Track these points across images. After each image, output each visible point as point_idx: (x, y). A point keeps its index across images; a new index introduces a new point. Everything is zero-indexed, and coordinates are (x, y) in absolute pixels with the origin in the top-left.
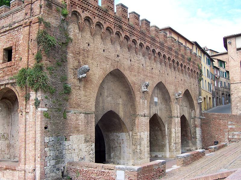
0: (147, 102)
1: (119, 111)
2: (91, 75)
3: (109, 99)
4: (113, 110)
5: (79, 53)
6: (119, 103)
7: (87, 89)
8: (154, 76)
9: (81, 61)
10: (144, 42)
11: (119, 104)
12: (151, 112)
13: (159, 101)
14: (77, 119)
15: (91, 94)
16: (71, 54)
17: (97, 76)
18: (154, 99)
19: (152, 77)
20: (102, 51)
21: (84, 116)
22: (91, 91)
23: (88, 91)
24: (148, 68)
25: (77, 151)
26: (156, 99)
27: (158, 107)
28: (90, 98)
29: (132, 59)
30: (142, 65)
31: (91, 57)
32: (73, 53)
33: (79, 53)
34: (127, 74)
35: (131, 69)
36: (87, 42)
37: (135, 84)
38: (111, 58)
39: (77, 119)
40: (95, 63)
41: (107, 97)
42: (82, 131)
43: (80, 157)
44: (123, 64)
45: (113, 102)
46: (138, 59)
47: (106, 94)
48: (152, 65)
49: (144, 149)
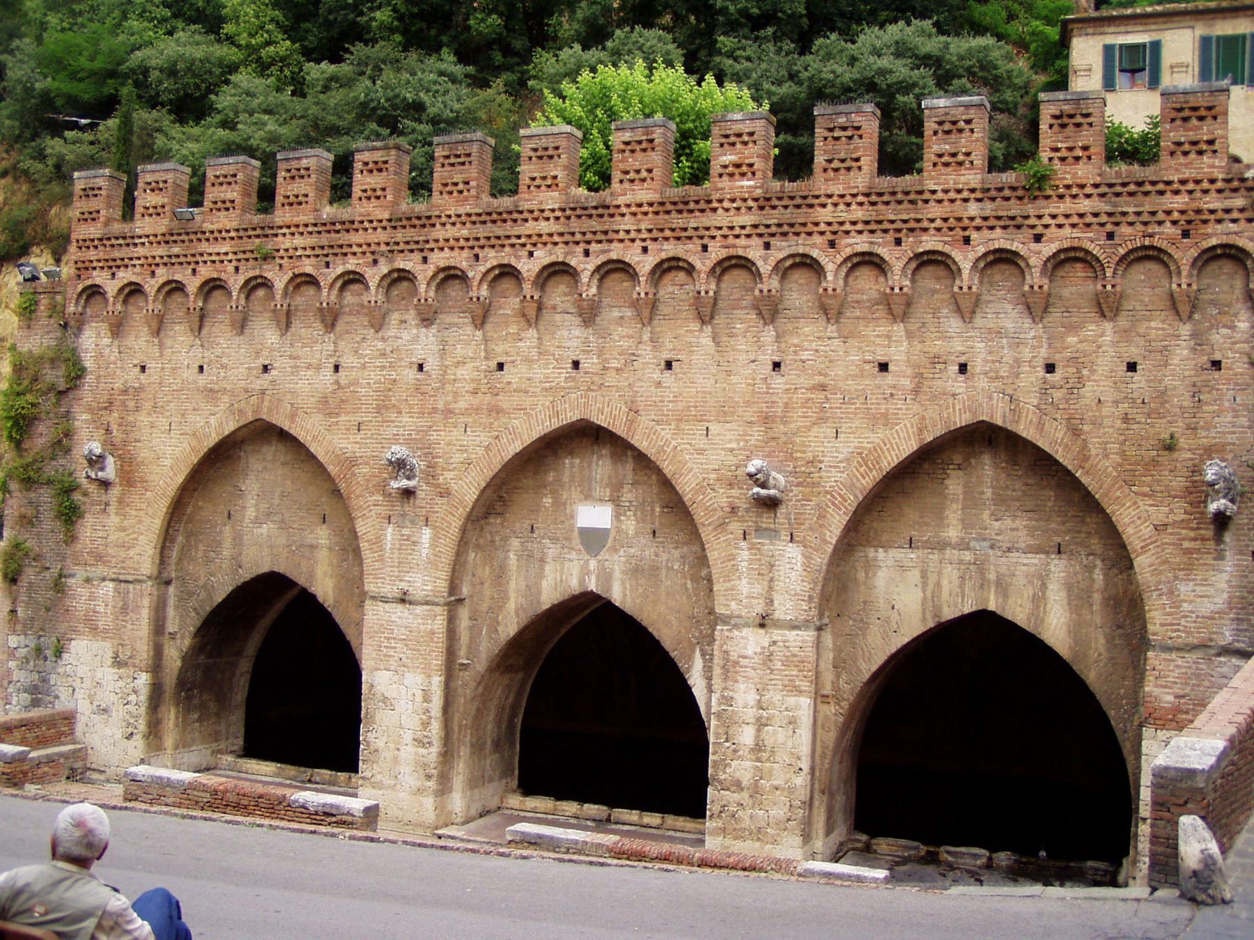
0: (435, 539)
1: (311, 575)
2: (146, 462)
3: (264, 529)
4: (281, 569)
5: (109, 406)
6: (314, 542)
7: (127, 509)
8: (504, 402)
9: (114, 427)
10: (417, 257)
11: (313, 547)
12: (544, 584)
13: (630, 524)
14: (92, 597)
15: (140, 522)
16: (84, 417)
17: (168, 462)
18: (572, 517)
19: (497, 411)
20: (190, 374)
21: (115, 590)
22: (142, 513)
23: (133, 513)
24: (465, 372)
25: (87, 683)
26: (594, 515)
27: (617, 562)
28: (135, 536)
29: (347, 360)
30: (412, 374)
31: (148, 405)
32: (90, 410)
33: (109, 406)
34: (307, 429)
35: (330, 406)
36: (136, 362)
37: (350, 462)
38: (228, 387)
39: (92, 597)
40: (163, 422)
41: (257, 521)
42: (105, 631)
43: (96, 703)
44: (289, 396)
45: (282, 540)
46: (389, 349)
47: (251, 513)
48: (500, 348)
49: (392, 746)
